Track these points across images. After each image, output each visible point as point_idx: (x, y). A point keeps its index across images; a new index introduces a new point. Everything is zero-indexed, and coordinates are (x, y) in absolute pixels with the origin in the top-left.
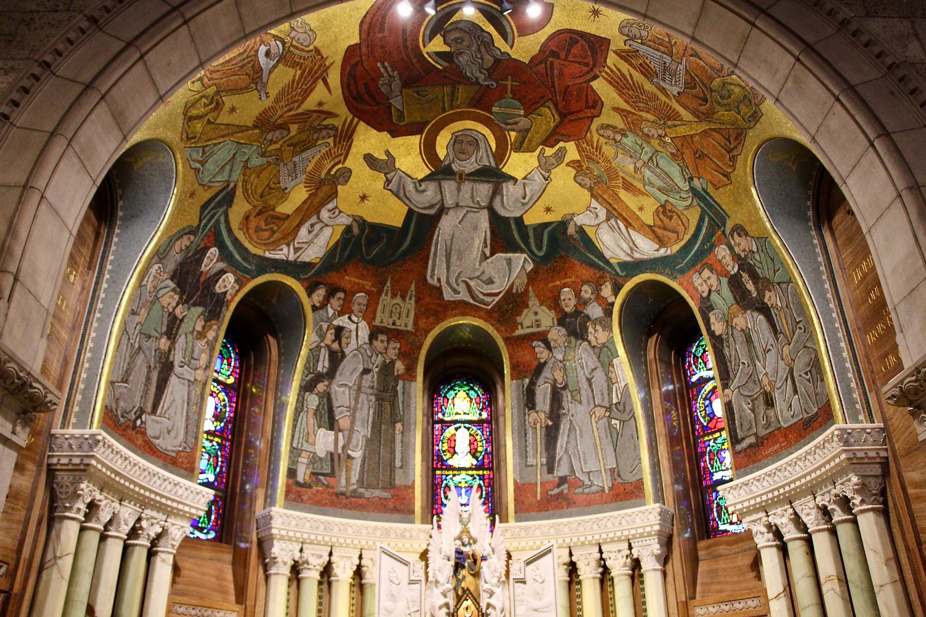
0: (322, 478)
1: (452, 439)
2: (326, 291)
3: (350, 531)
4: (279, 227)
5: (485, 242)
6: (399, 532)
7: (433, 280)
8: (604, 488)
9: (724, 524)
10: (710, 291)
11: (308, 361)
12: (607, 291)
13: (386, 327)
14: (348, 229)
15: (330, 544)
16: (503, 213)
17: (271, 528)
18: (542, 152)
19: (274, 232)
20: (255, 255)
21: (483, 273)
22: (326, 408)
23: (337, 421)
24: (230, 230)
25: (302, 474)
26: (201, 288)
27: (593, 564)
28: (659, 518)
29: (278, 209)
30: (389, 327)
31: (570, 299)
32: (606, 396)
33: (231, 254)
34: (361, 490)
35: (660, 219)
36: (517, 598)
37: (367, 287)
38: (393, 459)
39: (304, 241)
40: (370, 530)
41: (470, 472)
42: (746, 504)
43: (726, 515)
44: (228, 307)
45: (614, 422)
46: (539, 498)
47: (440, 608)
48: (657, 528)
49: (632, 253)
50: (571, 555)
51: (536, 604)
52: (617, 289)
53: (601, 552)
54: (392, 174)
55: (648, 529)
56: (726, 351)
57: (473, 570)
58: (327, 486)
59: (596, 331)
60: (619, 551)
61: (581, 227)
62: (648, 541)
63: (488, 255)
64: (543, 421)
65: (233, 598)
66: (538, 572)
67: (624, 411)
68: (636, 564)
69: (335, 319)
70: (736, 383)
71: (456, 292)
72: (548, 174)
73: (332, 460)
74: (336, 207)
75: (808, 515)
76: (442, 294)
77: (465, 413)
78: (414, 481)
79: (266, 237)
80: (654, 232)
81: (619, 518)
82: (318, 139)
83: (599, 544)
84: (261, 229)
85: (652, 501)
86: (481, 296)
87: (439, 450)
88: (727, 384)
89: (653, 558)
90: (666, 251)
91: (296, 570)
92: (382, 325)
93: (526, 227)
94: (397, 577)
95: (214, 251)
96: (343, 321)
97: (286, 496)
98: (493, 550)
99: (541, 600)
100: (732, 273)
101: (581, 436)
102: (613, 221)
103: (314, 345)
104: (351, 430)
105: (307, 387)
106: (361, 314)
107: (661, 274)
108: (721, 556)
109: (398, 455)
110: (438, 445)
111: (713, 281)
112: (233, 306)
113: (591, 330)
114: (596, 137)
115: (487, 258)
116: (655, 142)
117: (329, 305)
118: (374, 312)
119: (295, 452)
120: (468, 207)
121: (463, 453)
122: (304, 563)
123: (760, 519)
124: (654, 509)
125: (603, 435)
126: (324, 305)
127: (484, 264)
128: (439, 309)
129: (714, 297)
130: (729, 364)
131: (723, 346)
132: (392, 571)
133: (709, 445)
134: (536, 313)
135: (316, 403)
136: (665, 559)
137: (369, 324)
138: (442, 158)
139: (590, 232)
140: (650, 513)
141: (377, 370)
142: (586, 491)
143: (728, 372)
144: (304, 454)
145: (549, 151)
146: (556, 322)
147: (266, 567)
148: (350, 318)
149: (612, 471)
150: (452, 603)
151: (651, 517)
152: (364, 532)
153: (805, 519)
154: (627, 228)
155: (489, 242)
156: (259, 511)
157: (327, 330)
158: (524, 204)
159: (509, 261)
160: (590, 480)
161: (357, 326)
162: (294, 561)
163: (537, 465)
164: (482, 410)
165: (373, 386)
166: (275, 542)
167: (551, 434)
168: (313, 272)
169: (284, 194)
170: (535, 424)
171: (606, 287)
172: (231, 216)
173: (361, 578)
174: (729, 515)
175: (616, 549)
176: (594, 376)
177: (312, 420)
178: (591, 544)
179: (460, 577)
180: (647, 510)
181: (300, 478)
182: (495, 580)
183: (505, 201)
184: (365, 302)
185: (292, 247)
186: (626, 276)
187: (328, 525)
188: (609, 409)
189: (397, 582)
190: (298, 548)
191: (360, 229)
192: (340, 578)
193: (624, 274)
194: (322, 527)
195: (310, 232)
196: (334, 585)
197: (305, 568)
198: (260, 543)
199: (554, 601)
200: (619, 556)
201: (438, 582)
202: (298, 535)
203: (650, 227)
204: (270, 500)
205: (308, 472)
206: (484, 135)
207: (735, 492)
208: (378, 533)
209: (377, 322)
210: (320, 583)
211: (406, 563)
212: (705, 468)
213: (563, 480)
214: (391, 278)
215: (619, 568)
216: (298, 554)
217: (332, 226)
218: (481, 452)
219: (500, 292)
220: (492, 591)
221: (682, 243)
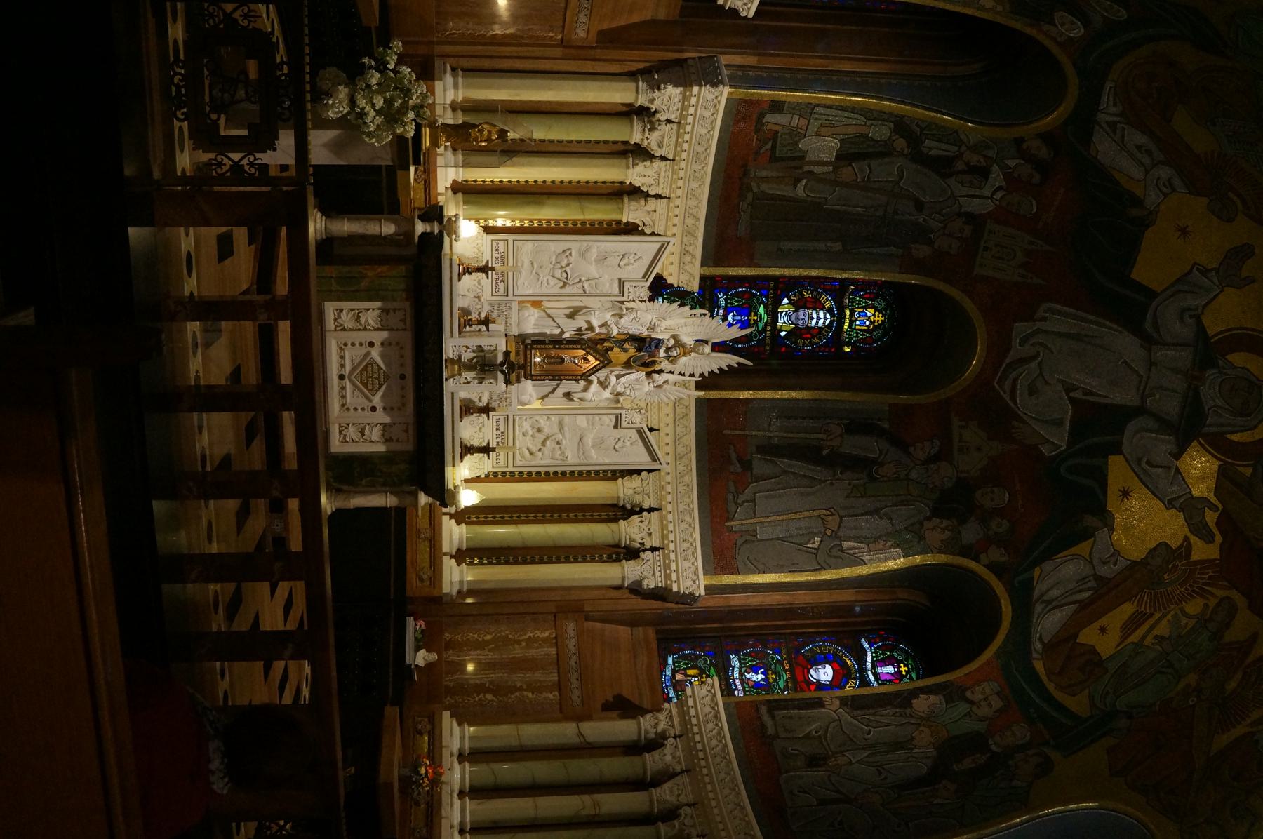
0: (769, 145)
1: (818, 306)
3: (694, 185)
5: (1091, 393)
6: (691, 248)
7: (1045, 312)
8: (732, 520)
9: (674, 662)
10: (972, 703)
12: (996, 555)
14: (1138, 202)
15: (677, 158)
16: (1131, 427)
17: (700, 85)
18: (1213, 508)
21: (1046, 383)
22: (871, 150)
23: (850, 165)
25: (775, 121)
27: (637, 499)
28: (687, 592)
31: (992, 500)
32: (852, 533)
34: (750, 196)
36: (597, 418)
40: (694, 211)
41: (769, 328)
42: (692, 712)
43: (685, 666)
45: (817, 540)
46: (726, 432)
47: (588, 322)
48: (675, 589)
49: (1044, 602)
51: (589, 440)
53: (651, 510)
54: (1216, 280)
55: (674, 577)
57: (634, 362)
58: (757, 153)
59: (943, 530)
60: (650, 534)
61: (1093, 535)
62: (659, 574)
63: (1072, 394)
64: (828, 443)
65: (606, 26)
66: (628, 443)
67: (831, 556)
68: (632, 553)
71: (1024, 341)
72: (1177, 506)
73: (794, 159)
74: (1174, 190)
75: (671, 791)
77: (851, 323)
78: (759, 266)
81: (691, 540)
83: (661, 509)
85: (707, 583)
86: (1014, 374)
87: (804, 286)
88: (846, 704)
89: (638, 578)
90: (1037, 651)
91: (644, 113)
93: (1106, 457)
94: (628, 264)
96: (997, 177)
97: (745, 101)
98: (659, 387)
99: (593, 446)
100: (990, 742)
101: (802, 494)
102: (1092, 584)
103: (963, 137)
105: (900, 125)
110: (809, 285)
111: (984, 711)
112: (1028, 30)
113: (945, 523)
114: (1221, 593)
115: (1068, 391)
116: (1192, 679)
119: (807, 110)
120: (1149, 377)
121: (797, 318)
122: (652, 123)
123: (673, 726)
124: (699, 587)
127: (1060, 387)
129: (963, 707)
130: (871, 711)
131: (896, 707)
132: (637, 257)
133: (774, 653)
134: (979, 449)
135: (877, 137)
136: (636, 590)
138: (1229, 357)
139: (1083, 548)
140: (694, 582)
141: (921, 220)
142: (731, 497)
143: (862, 708)
144: (803, 122)
145: (1211, 517)
146: (964, 475)
148: (1000, 188)
151: (689, 583)
152: (692, 203)
153: (666, 786)
155: (1091, 399)
156: (724, 59)
157: (985, 156)
158: (1139, 461)
159: (1059, 423)
160: (744, 502)
161: (989, 198)
162: (656, 112)
163: (769, 431)
164: (853, 345)
165: (897, 214)
166: (680, 89)
167: (808, 453)
170: (826, 431)
174: (685, 669)
175: (652, 530)
176: (881, 518)
177: (851, 130)
178: (661, 498)
179: (626, 346)
180: (698, 578)
181: (769, 118)
182: (620, 389)
183: (1148, 434)
187: (702, 157)
188: (836, 535)
189: (622, 264)
190: (673, 117)
192: (630, 171)
194: (700, 149)
195: (1139, 147)
197: (645, 126)
198: (680, 63)
199: (593, 462)
200: (644, 534)
201: (621, 318)
202: (690, 119)
203: (1076, 636)
204: (739, 78)
205: (777, 128)
206: (1255, 427)
207: (708, 700)
208: (689, 221)
210: (626, 143)
212: (746, 645)
213: (747, 465)
215: (631, 530)
216: (663, 118)
217: (1145, 179)
218: (796, 343)
219: (1015, 404)
220: (607, 387)
221: (1044, 678)
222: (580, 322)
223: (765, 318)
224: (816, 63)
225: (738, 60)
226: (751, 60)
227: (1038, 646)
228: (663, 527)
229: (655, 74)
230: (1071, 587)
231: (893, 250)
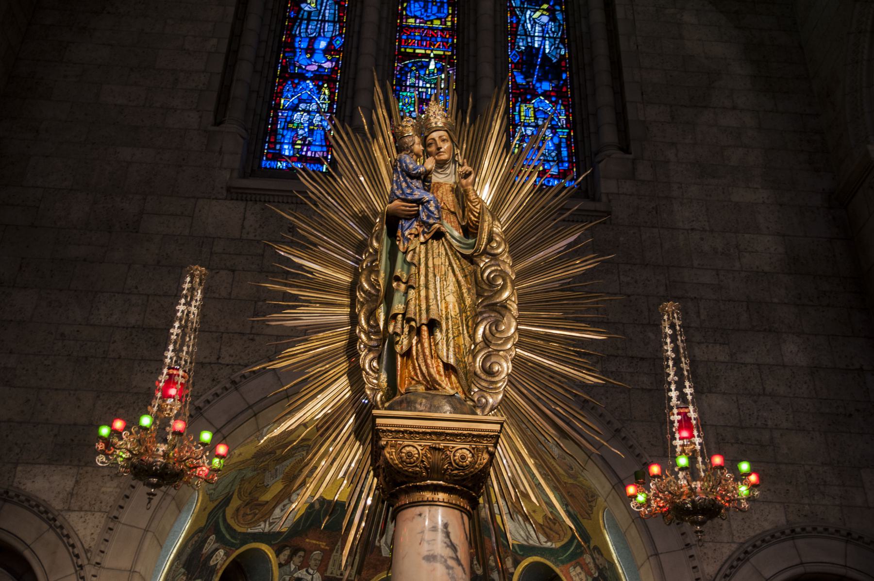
2: (291, 551)
4: (260, 511)
13: (335, 577)
19: (255, 514)
20: (240, 532)
24: (225, 520)
26: (201, 565)
29: (260, 500)
30: (338, 577)
33: (224, 536)
35: (548, 522)
37: (323, 547)
39: (278, 517)
44: (217, 573)
52: (516, 563)
69: (296, 572)
76: (380, 551)
79: (249, 519)
80: (543, 529)
82: (295, 453)
84: (247, 514)
90: (552, 545)
92: (332, 575)
95: (213, 537)
106: (316, 568)
107: (548, 559)
112: (220, 574)
117: (292, 562)
118: (327, 566)
126: (288, 562)
128: (378, 563)
137: (322, 575)
148: (307, 571)
154: (524, 521)
161: (312, 577)
168: (282, 538)
169: (265, 488)
171: (508, 560)
172: (227, 512)
184: (320, 558)
185: (267, 523)
186: (523, 555)
191: (320, 505)
193: (522, 553)
195: (282, 510)
209: (328, 574)
214: (342, 539)
221: (563, 543)
227: (549, 544)
230: (518, 525)
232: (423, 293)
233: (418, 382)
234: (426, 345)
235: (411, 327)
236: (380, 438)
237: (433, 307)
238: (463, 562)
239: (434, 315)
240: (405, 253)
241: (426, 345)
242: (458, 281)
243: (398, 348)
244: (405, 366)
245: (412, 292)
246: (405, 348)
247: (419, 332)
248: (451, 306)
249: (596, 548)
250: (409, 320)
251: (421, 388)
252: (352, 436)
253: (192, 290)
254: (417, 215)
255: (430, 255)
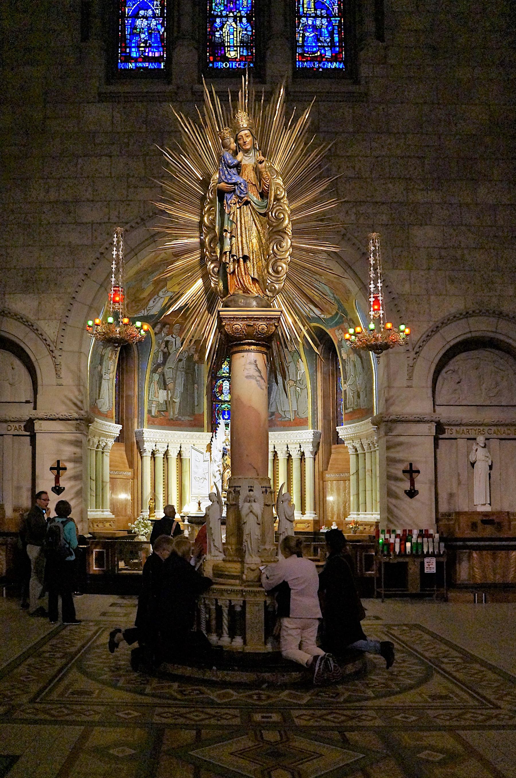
3: (176, 436)
11: (153, 358)
25: (154, 412)
27: (284, 452)
38: (194, 402)
50: (274, 448)
56: (346, 367)
65: (128, 466)
68: (303, 454)
70: (348, 383)
104: (174, 389)
105: (154, 371)
108: (341, 453)
109: (196, 399)
119: (150, 402)
125: (292, 394)
136: (315, 453)
144: (154, 403)
147: (141, 453)
149: (295, 411)
150: (222, 470)
152: (182, 436)
156: (136, 429)
173: (181, 456)
177: (156, 386)
178: (283, 444)
181: (153, 414)
188: (295, 382)
196: (169, 460)
204: (141, 424)
208: (188, 437)
210: (164, 458)
211: (202, 453)
215: (295, 456)
222: (217, 474)
223: (226, 405)
224: (136, 400)
225: (136, 425)
226: (136, 420)
228: (293, 443)
229: (141, 452)
231: (196, 367)
232: (240, 239)
233: (239, 289)
234: (243, 269)
235: (234, 260)
236: (222, 322)
237: (245, 248)
238: (264, 377)
239: (246, 253)
240: (229, 214)
241: (243, 269)
242: (258, 230)
243: (228, 270)
244: (232, 278)
245: (234, 239)
246: (231, 270)
247: (238, 261)
248: (254, 245)
249: (351, 320)
250: (233, 256)
251: (241, 292)
252: (207, 312)
253: (118, 242)
254: (234, 191)
255: (242, 216)
